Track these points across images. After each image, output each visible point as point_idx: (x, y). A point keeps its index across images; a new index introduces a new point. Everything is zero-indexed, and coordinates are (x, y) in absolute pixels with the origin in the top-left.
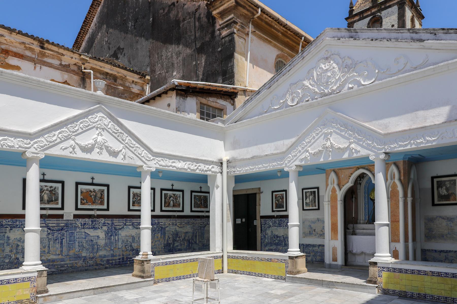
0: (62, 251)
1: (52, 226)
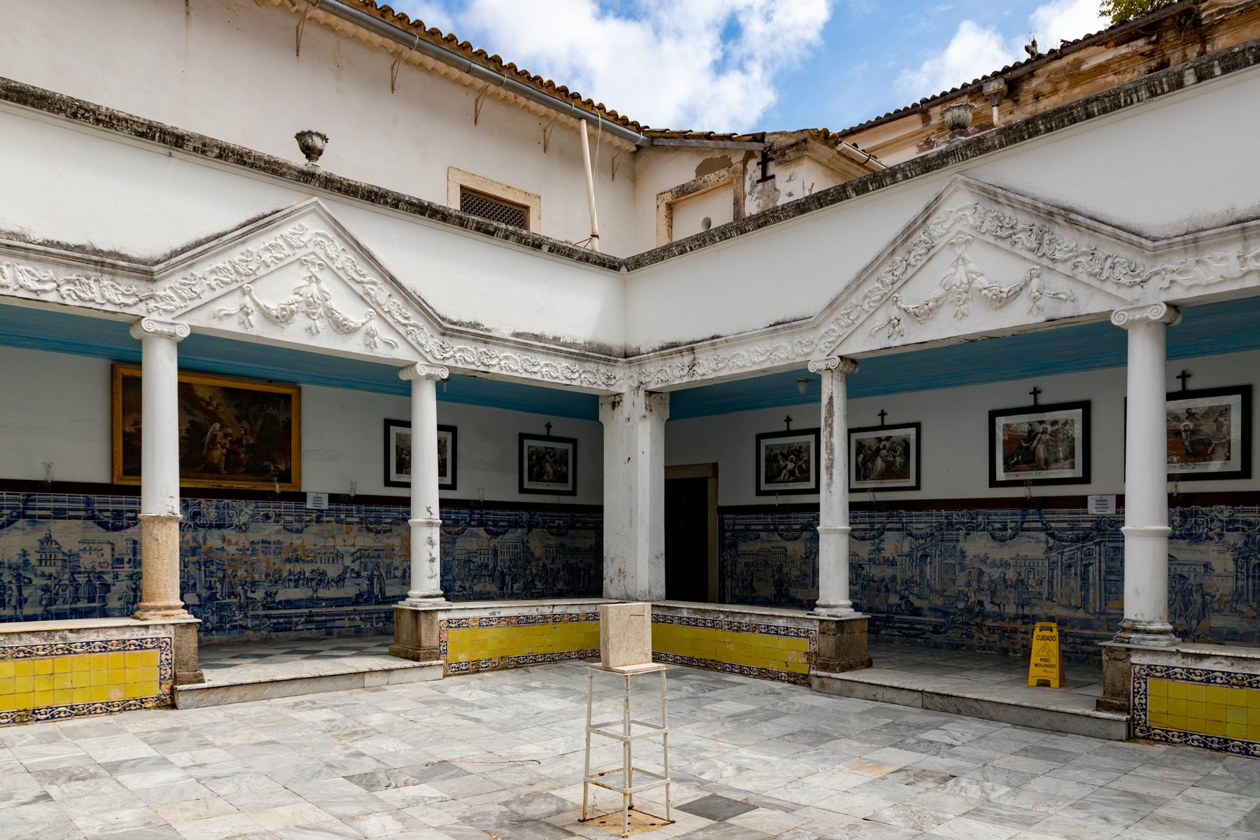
0: (1085, 599)
1: (1057, 529)
